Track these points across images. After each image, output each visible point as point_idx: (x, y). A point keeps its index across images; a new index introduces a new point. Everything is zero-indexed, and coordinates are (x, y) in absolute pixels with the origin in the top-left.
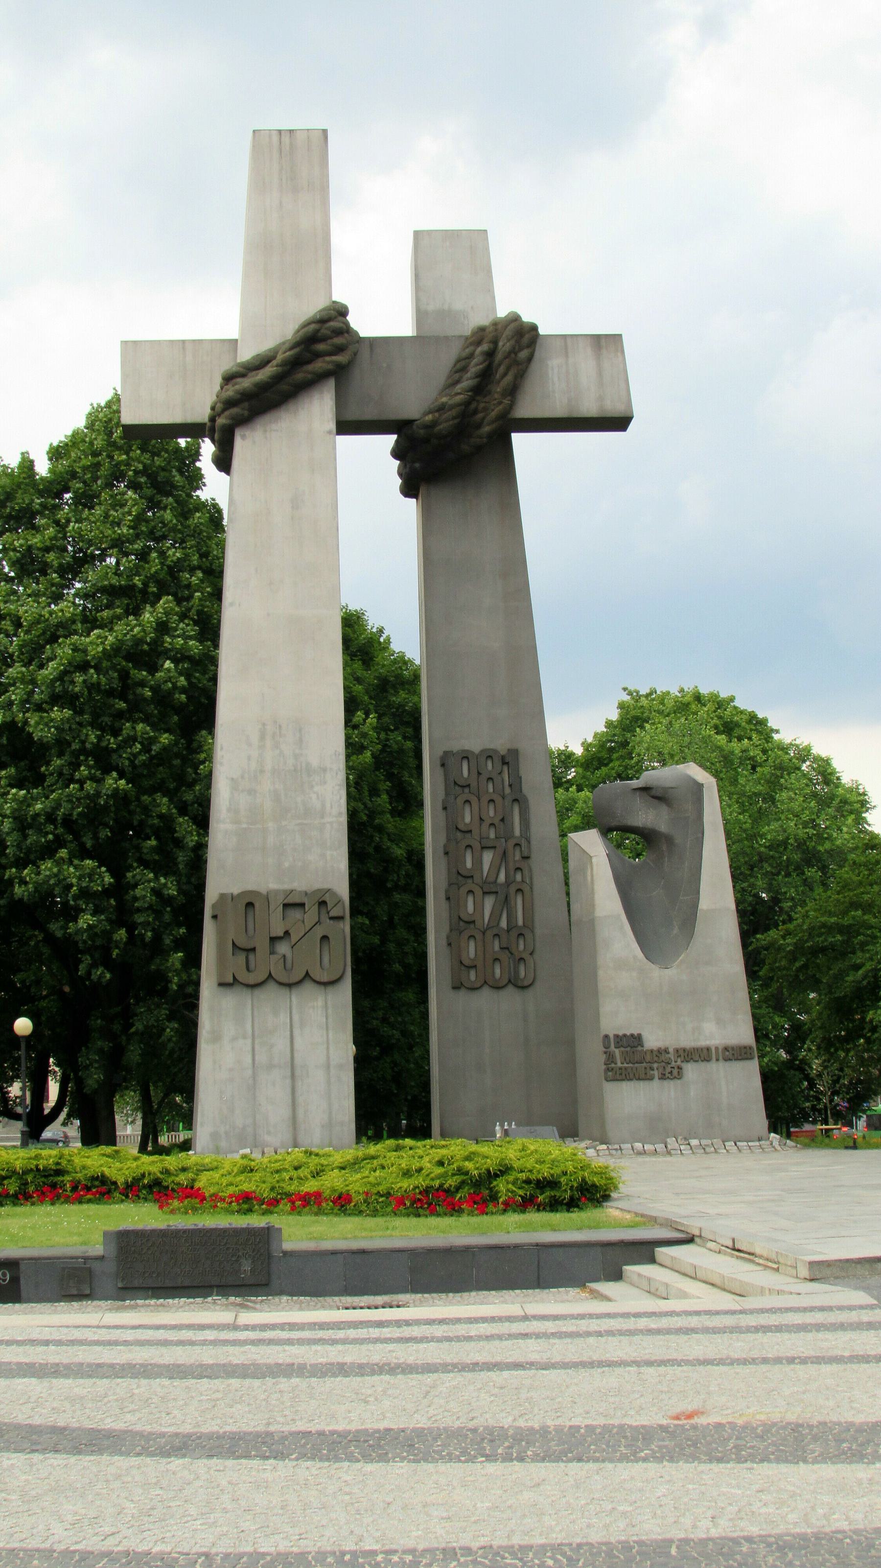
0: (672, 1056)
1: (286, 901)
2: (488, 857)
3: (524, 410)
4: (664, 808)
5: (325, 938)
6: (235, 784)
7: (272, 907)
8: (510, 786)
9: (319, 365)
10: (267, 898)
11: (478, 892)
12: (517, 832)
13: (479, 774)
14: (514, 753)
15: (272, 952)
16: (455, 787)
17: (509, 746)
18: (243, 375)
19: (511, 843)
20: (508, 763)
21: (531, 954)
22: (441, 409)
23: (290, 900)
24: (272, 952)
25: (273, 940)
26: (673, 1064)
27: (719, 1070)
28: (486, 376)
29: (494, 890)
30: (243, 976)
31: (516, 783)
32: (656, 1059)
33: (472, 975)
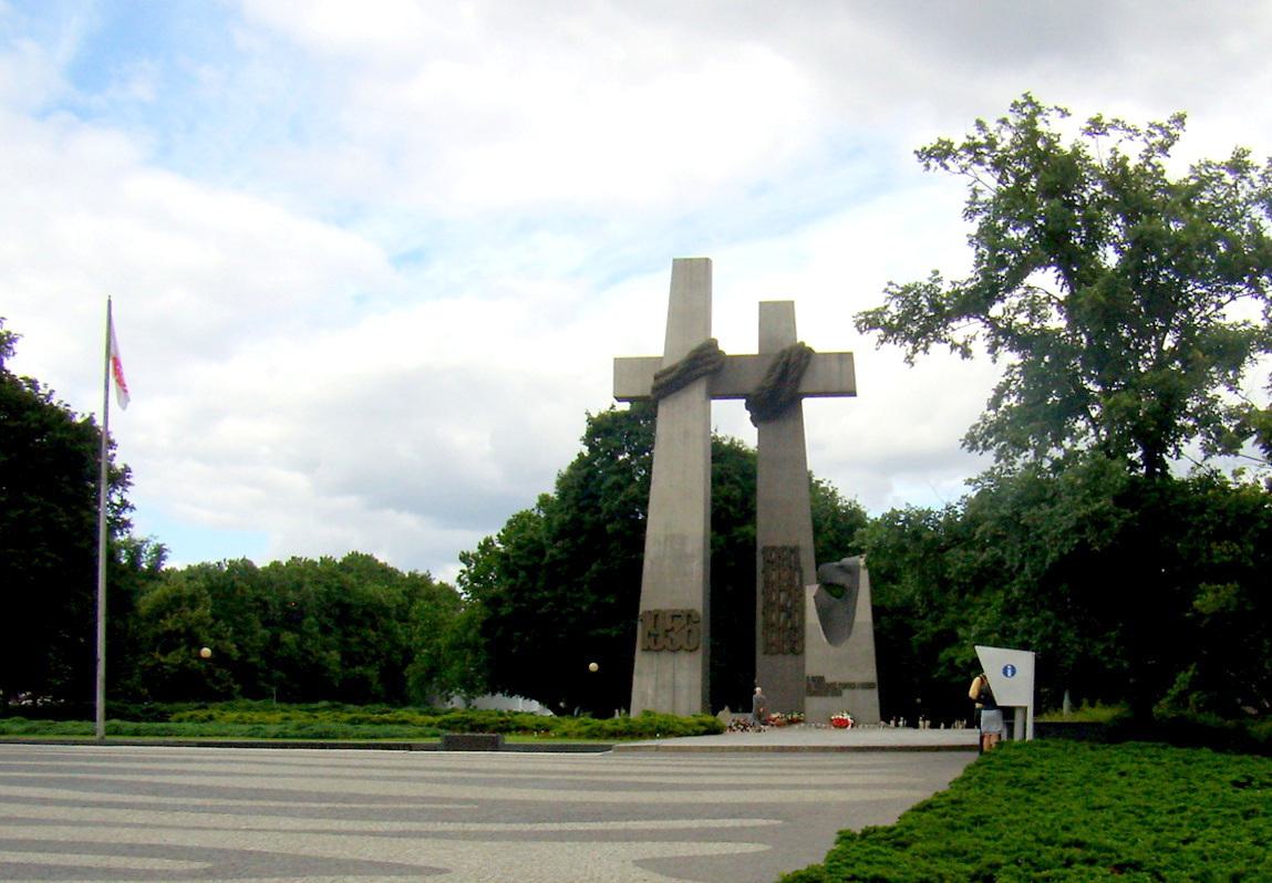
2: (783, 596)
3: (803, 389)
5: (689, 631)
6: (652, 563)
9: (699, 371)
10: (664, 613)
12: (797, 583)
15: (666, 636)
16: (769, 562)
22: (763, 388)
24: (666, 636)
25: (667, 631)
28: (785, 373)
31: (798, 562)
33: (773, 648)
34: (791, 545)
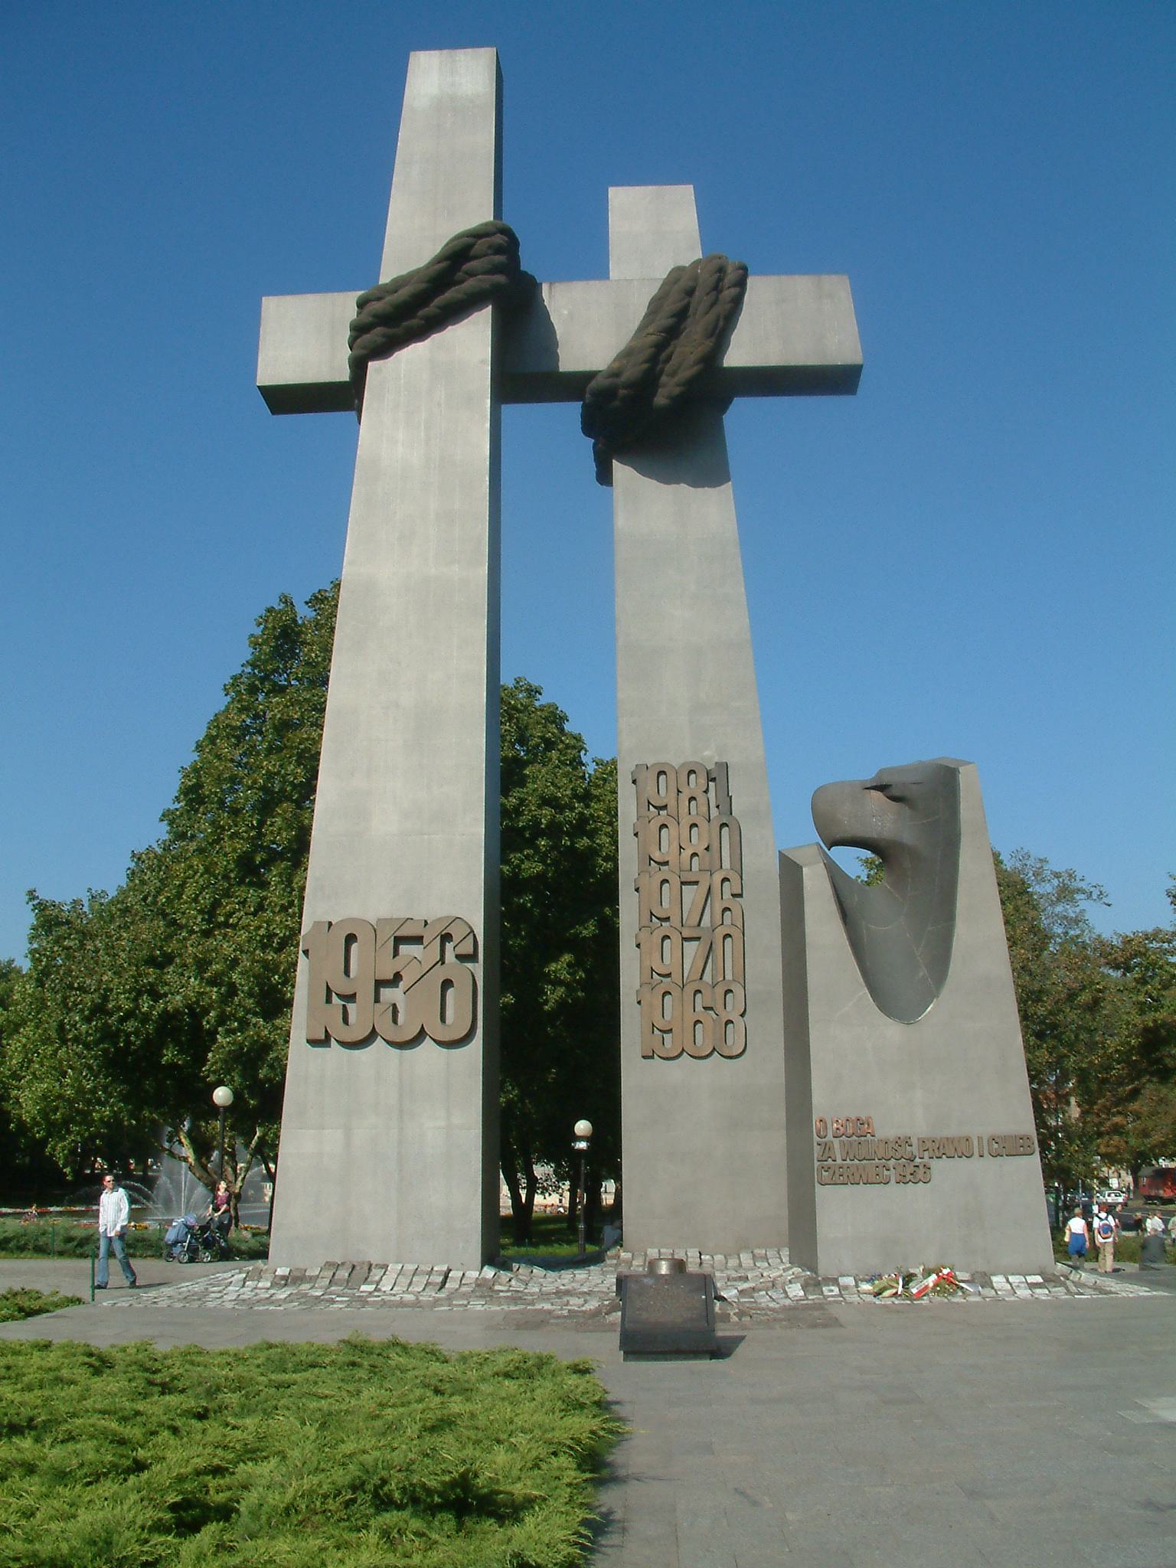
0: (915, 1149)
1: (398, 934)
7: (379, 944)
11: (676, 938)
14: (725, 767)
17: (716, 759)
18: (379, 299)
19: (718, 877)
20: (714, 780)
21: (742, 1015)
23: (404, 932)
24: (377, 1000)
25: (380, 984)
26: (918, 1160)
27: (983, 1169)
30: (339, 1031)
31: (726, 803)
32: (892, 1153)
34: (709, 756)
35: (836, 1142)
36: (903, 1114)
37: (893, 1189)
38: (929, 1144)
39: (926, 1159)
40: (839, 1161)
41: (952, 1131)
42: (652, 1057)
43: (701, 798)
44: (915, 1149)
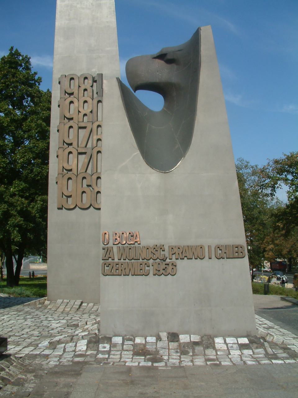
0: (166, 253)
4: (174, 66)
8: (97, 93)
11: (75, 153)
13: (79, 86)
14: (101, 76)
26: (168, 260)
27: (211, 267)
29: (83, 151)
32: (151, 255)
34: (94, 71)
35: (115, 249)
36: (159, 229)
37: (151, 279)
38: (176, 250)
39: (174, 260)
40: (116, 260)
41: (192, 241)
42: (62, 209)
43: (90, 89)
44: (166, 253)
